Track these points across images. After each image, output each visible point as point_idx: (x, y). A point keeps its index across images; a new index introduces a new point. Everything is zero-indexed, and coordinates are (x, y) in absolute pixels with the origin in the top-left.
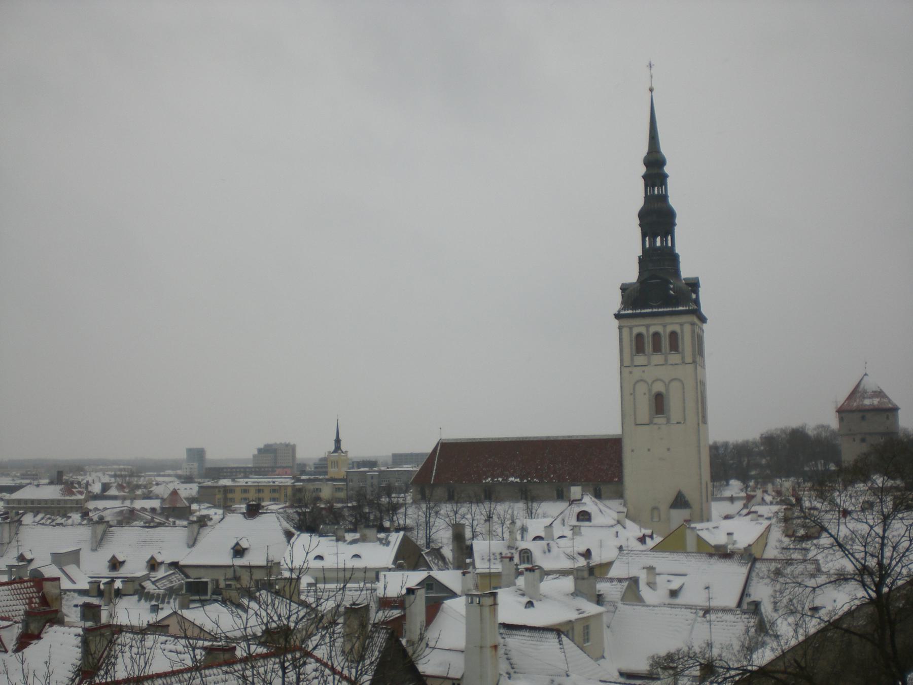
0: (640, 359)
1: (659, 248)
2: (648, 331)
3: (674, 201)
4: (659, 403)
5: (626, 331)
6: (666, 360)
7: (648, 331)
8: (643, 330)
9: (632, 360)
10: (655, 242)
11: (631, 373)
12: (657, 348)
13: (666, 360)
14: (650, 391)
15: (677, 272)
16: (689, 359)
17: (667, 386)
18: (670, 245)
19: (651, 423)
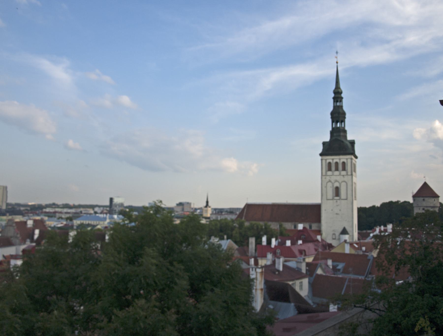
0: (329, 173)
1: (339, 128)
2: (333, 161)
3: (345, 108)
4: (337, 192)
5: (324, 161)
6: (340, 173)
7: (333, 161)
8: (331, 161)
9: (326, 173)
10: (337, 125)
11: (325, 178)
12: (337, 169)
13: (340, 173)
14: (333, 186)
15: (346, 137)
16: (349, 173)
17: (340, 184)
18: (343, 126)
19: (333, 199)
